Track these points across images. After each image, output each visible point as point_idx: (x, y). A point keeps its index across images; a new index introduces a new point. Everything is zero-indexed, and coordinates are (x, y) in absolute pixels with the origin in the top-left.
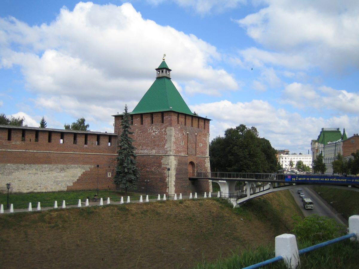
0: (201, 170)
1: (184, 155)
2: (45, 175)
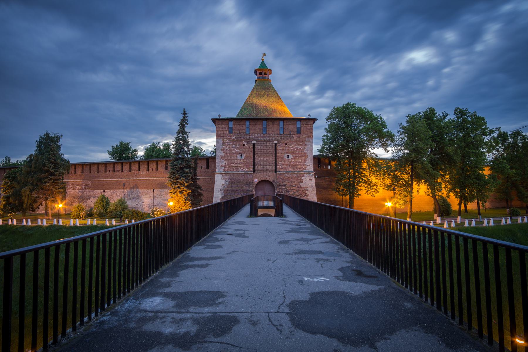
0: (289, 191)
1: (243, 172)
2: (161, 198)
